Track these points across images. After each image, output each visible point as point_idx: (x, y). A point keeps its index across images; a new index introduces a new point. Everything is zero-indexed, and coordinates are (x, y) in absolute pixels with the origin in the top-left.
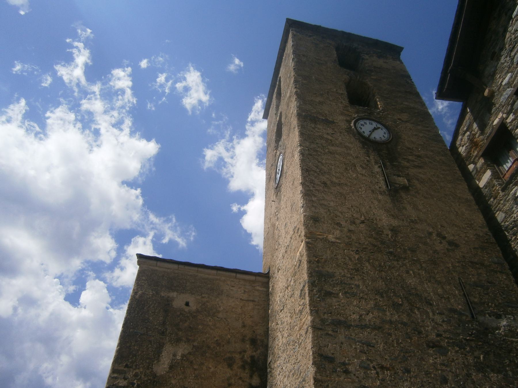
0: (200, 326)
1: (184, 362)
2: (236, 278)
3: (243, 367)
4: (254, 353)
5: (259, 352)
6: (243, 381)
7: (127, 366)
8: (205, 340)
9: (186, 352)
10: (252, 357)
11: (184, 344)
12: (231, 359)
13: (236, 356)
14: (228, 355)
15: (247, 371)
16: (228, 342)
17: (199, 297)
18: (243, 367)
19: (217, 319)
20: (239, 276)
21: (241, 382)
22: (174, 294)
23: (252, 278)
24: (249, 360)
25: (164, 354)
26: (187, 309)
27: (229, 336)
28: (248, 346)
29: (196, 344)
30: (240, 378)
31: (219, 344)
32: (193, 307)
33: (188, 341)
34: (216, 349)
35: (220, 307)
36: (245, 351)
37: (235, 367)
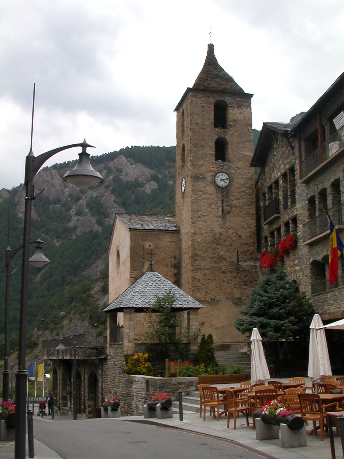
2: (167, 232)
4: (175, 262)
5: (176, 261)
7: (134, 270)
10: (174, 263)
12: (167, 265)
15: (173, 268)
16: (166, 259)
18: (171, 267)
20: (168, 231)
22: (144, 243)
23: (173, 232)
24: (173, 265)
25: (145, 265)
29: (155, 260)
32: (152, 247)
37: (169, 267)
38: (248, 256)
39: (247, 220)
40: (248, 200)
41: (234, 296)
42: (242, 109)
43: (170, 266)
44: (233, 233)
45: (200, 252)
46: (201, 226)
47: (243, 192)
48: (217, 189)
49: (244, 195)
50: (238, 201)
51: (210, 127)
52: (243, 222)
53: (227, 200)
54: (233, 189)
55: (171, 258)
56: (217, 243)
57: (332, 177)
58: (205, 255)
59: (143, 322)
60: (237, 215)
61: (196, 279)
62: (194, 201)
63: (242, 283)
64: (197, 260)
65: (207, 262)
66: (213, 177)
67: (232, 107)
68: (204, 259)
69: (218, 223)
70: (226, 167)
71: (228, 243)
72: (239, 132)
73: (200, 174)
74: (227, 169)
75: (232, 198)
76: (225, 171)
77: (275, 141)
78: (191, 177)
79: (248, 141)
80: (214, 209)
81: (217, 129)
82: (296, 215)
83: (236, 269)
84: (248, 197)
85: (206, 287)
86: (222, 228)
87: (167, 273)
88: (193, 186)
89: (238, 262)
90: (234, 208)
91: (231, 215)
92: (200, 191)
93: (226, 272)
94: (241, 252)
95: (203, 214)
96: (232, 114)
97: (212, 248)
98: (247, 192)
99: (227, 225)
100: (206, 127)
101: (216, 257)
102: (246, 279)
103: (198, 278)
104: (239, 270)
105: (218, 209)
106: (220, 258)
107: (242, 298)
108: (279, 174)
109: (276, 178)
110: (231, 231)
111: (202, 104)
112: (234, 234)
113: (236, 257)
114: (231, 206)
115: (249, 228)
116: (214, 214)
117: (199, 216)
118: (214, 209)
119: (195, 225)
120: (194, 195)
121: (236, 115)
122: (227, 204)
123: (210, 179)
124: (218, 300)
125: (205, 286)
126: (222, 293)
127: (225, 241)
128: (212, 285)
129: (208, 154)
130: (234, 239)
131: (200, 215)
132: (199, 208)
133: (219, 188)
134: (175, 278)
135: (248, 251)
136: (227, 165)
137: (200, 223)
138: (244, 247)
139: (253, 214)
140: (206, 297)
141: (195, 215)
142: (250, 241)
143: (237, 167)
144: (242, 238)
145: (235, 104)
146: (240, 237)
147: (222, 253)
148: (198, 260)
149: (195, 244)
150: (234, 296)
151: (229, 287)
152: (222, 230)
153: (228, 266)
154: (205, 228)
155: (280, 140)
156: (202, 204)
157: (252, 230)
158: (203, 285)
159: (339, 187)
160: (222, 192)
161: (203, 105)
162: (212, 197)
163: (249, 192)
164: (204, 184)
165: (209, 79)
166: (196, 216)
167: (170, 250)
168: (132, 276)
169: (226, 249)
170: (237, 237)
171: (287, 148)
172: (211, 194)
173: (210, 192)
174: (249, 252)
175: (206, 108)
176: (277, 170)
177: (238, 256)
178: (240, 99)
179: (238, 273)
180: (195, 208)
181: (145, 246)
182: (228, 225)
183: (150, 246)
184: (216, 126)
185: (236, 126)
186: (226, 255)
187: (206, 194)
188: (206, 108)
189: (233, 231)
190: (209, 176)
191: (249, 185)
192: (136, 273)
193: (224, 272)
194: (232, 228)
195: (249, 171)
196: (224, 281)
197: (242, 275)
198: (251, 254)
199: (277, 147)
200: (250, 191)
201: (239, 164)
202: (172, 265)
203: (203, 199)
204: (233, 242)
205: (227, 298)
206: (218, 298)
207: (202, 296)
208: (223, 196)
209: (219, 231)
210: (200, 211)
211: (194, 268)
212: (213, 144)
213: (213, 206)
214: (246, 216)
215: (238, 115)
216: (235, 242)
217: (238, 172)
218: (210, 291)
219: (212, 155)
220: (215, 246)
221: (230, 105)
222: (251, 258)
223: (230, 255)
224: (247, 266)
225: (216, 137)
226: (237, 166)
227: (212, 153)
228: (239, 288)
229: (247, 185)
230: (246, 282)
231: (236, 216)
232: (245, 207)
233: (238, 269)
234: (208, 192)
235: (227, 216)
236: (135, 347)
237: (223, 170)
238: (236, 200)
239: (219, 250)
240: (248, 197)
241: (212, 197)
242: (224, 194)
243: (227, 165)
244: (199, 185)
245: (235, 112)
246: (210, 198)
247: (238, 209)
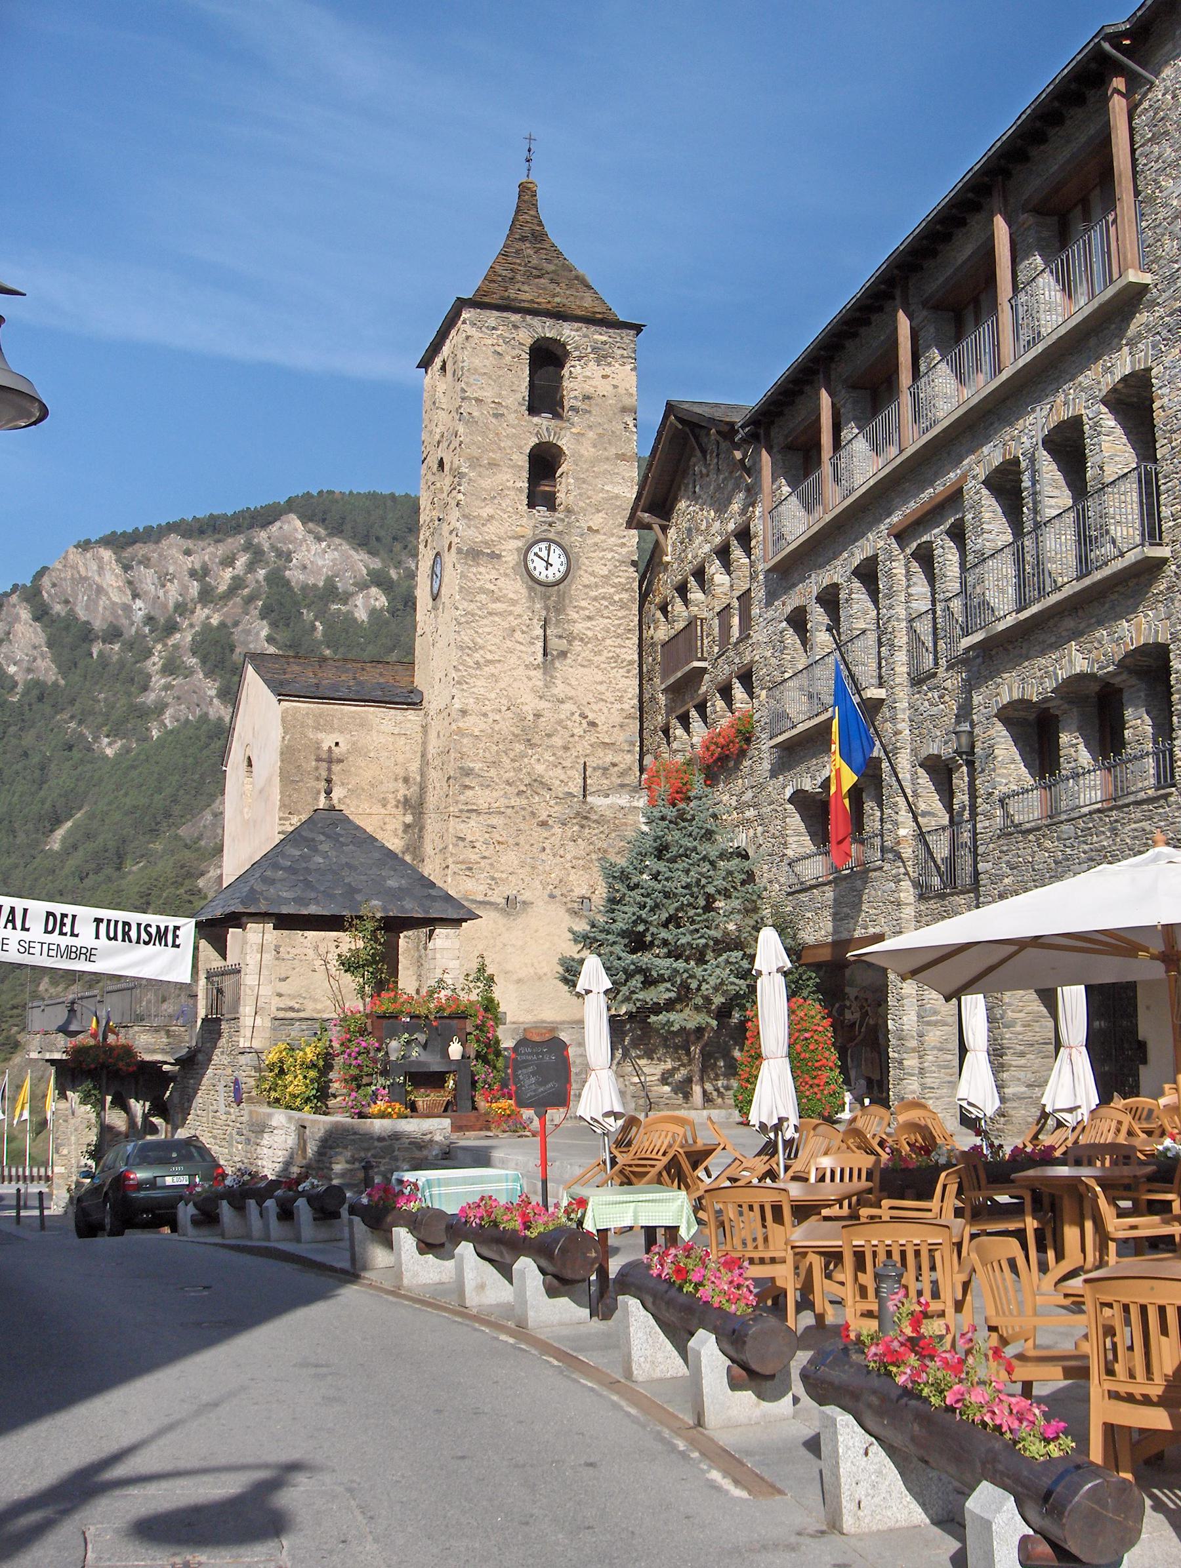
9: (342, 796)
10: (405, 796)
18: (397, 807)
22: (321, 736)
24: (402, 799)
33: (343, 784)
37: (389, 806)
38: (613, 779)
39: (615, 678)
40: (617, 622)
41: (572, 891)
42: (609, 364)
44: (573, 714)
45: (477, 766)
46: (482, 691)
47: (603, 598)
48: (531, 589)
49: (607, 607)
50: (589, 624)
51: (516, 411)
52: (601, 683)
53: (558, 621)
54: (575, 588)
55: (396, 780)
56: (529, 740)
57: (856, 551)
58: (493, 772)
60: (586, 663)
61: (463, 839)
62: (463, 620)
63: (594, 856)
64: (467, 787)
65: (495, 794)
66: (519, 555)
67: (580, 358)
68: (489, 786)
69: (530, 684)
70: (559, 527)
71: (557, 741)
72: (601, 431)
73: (486, 543)
74: (560, 533)
75: (575, 616)
76: (557, 539)
77: (698, 453)
78: (459, 551)
79: (623, 454)
80: (521, 643)
81: (536, 420)
82: (752, 662)
83: (578, 814)
84: (620, 614)
85: (491, 865)
86: (541, 698)
88: (463, 576)
89: (584, 796)
90: (577, 643)
91: (569, 661)
92: (482, 590)
93: (550, 822)
94: (594, 769)
95: (489, 657)
96: (580, 378)
97: (512, 754)
98: (616, 598)
99: (555, 691)
100: (505, 412)
101: (521, 780)
102: (605, 846)
103: (469, 838)
104: (586, 818)
105: (533, 644)
106: (536, 784)
107: (594, 897)
108: (707, 548)
109: (699, 559)
110: (568, 706)
111: (497, 348)
112: (576, 717)
113: (581, 782)
114: (571, 638)
115: (620, 700)
116: (519, 658)
117: (477, 663)
118: (521, 643)
119: (465, 687)
120: (466, 604)
121: (593, 383)
122: (559, 631)
123: (511, 559)
124: (524, 902)
125: (489, 861)
126: (538, 882)
127: (549, 736)
128: (510, 858)
129: (509, 489)
130: (576, 731)
131: (482, 661)
132: (479, 640)
133: (537, 586)
135: (614, 765)
136: (563, 520)
137: (479, 683)
138: (601, 755)
139: (631, 663)
140: (490, 893)
141: (467, 658)
142: (620, 737)
143: (590, 529)
144: (599, 729)
145: (589, 350)
146: (593, 724)
147: (540, 768)
148: (472, 788)
149: (465, 741)
150: (572, 891)
151: (556, 864)
152: (543, 704)
153: (556, 808)
154: (493, 696)
155: (712, 453)
156: (487, 630)
157: (626, 706)
158: (485, 858)
159: (877, 579)
160: (546, 598)
161: (499, 349)
162: (518, 610)
163: (621, 600)
164: (494, 572)
165: (519, 277)
166: (470, 662)
168: (284, 828)
169: (552, 759)
170: (585, 725)
171: (731, 473)
172: (514, 602)
173: (511, 595)
174: (616, 769)
175: (508, 358)
176: (701, 538)
177: (585, 779)
178: (604, 338)
179: (582, 827)
180: (466, 638)
182: (559, 689)
183: (337, 744)
184: (533, 410)
185: (589, 412)
186: (554, 776)
187: (498, 600)
188: (508, 358)
189: (574, 708)
190: (510, 551)
191: (623, 580)
193: (543, 824)
194: (571, 698)
195: (624, 540)
196: (544, 849)
197: (596, 831)
198: (622, 774)
199: (704, 471)
200: (625, 596)
201: (596, 521)
202: (399, 801)
203: (490, 614)
204: (571, 739)
205: (552, 896)
206: (526, 896)
207: (481, 888)
208: (547, 608)
209: (532, 705)
210: (481, 648)
211: (461, 811)
212: (523, 461)
213: (518, 635)
214: (613, 668)
215: (598, 382)
216: (576, 738)
217: (590, 542)
218: (504, 876)
219: (520, 490)
220: (519, 747)
221: (577, 353)
222: (622, 786)
223: (563, 777)
224: (610, 807)
225: (534, 441)
226: (591, 524)
227: (521, 484)
228: (584, 868)
229: (616, 581)
230: (605, 851)
231: (583, 666)
232: (608, 642)
233: (584, 818)
234: (505, 596)
235: (557, 664)
236: (274, 1029)
237: (551, 536)
238: (584, 619)
239: (532, 761)
240: (620, 614)
241: (518, 610)
242: (551, 603)
243: (563, 520)
244: (480, 573)
245: (589, 374)
246: (511, 613)
247: (589, 645)
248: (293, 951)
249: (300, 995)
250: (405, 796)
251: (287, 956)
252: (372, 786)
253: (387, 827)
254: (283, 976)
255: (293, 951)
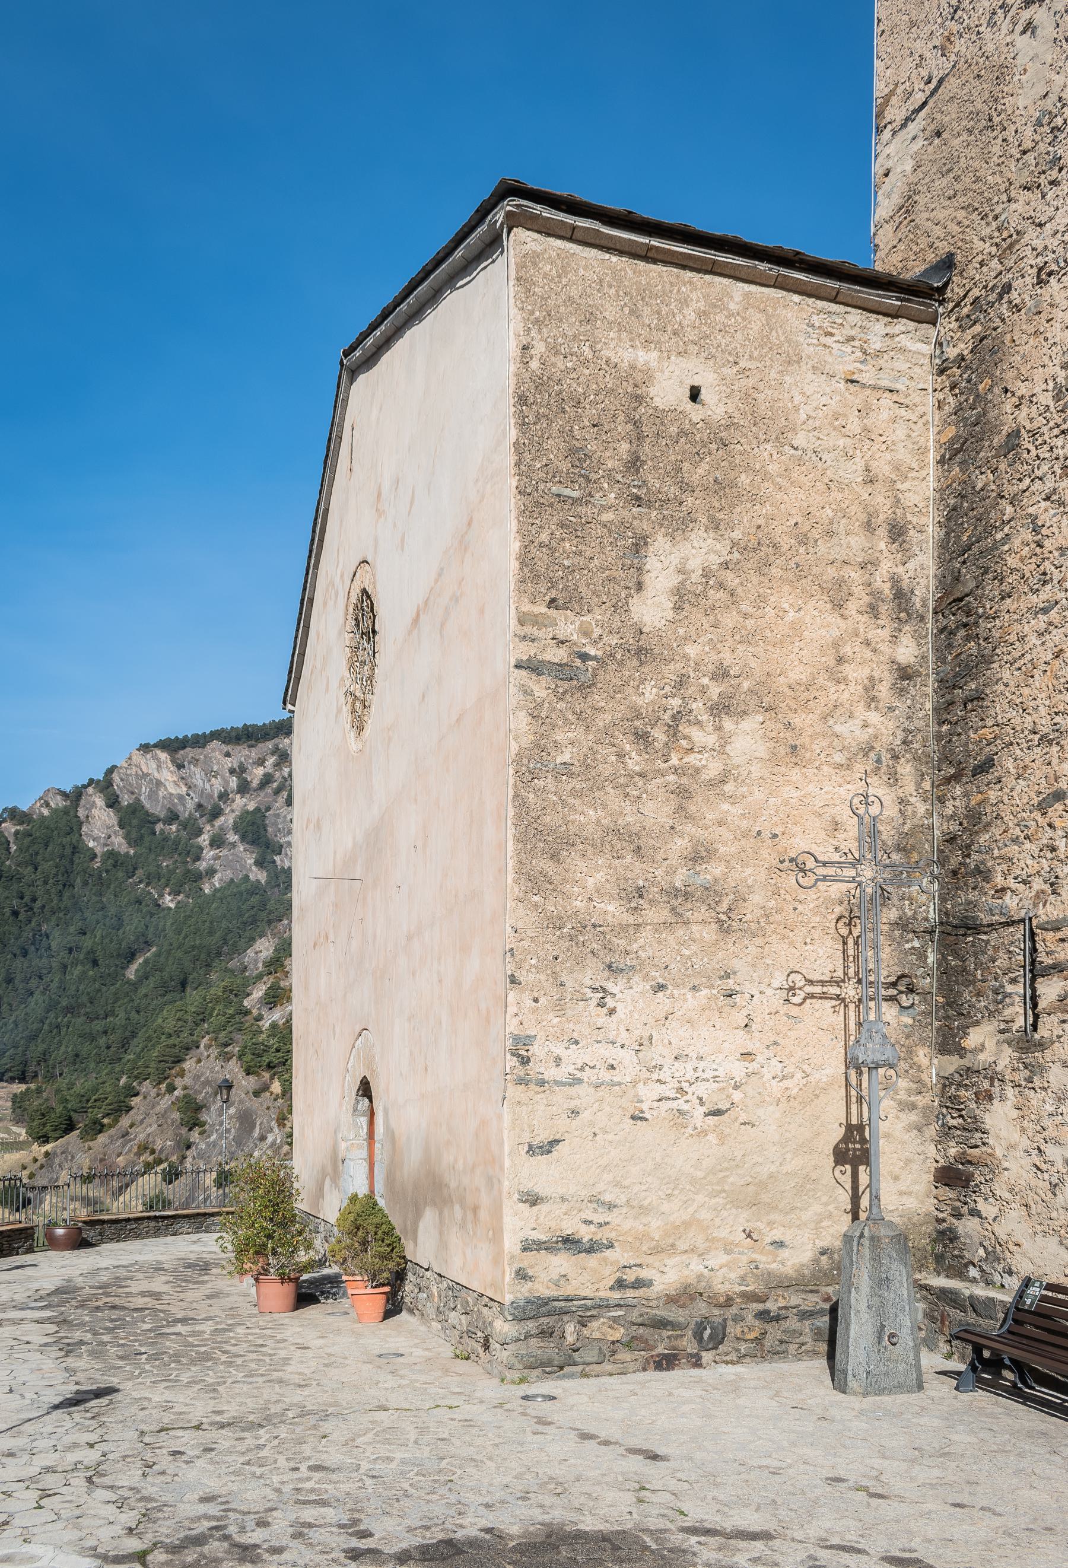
0: (743, 476)
1: (712, 592)
3: (873, 611)
4: (900, 569)
6: (875, 651)
8: (761, 521)
9: (714, 560)
10: (895, 580)
11: (705, 535)
12: (840, 583)
13: (853, 574)
14: (831, 572)
17: (730, 372)
18: (873, 611)
19: (792, 452)
21: (868, 654)
24: (887, 589)
26: (695, 412)
27: (829, 512)
28: (882, 545)
29: (737, 535)
30: (867, 642)
31: (804, 540)
33: (715, 525)
34: (797, 551)
35: (797, 409)
36: (875, 563)
37: (852, 607)
43: (860, 599)
59: (635, 1083)
87: (840, 660)
134: (901, 706)
167: (859, 464)
181: (652, 391)
183: (695, 394)
192: (567, 625)
202: (876, 595)
248: (574, 1057)
249: (596, 1201)
250: (895, 580)
251: (551, 1073)
252: (804, 540)
253: (848, 669)
254: (543, 1136)
255: (574, 1057)
